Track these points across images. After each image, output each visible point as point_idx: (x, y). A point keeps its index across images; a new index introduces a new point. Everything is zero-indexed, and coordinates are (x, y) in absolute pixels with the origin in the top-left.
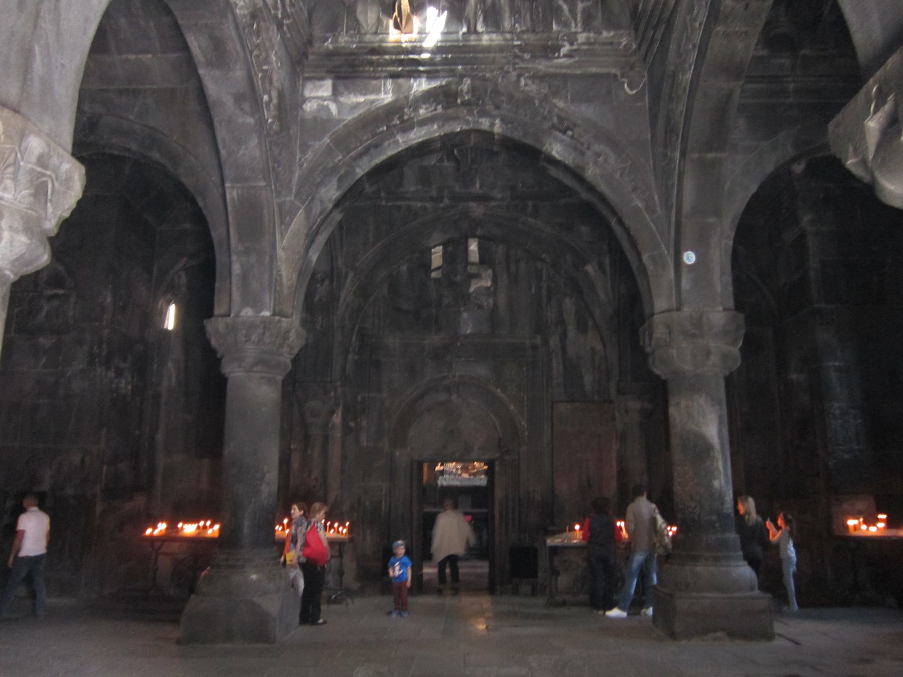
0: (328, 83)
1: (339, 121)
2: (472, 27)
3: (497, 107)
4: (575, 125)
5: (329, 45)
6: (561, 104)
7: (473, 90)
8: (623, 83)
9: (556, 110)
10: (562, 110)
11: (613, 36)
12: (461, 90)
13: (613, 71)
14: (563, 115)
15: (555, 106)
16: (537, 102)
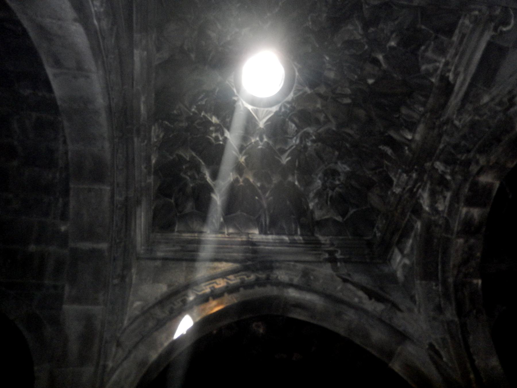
0: (396, 251)
1: (413, 264)
2: (407, 142)
3: (468, 151)
4: (510, 92)
5: (378, 234)
6: (486, 99)
7: (446, 163)
8: (502, 32)
9: (492, 104)
10: (493, 99)
11: (460, 32)
12: (442, 171)
13: (487, 37)
14: (497, 100)
15: (487, 104)
16: (477, 118)
